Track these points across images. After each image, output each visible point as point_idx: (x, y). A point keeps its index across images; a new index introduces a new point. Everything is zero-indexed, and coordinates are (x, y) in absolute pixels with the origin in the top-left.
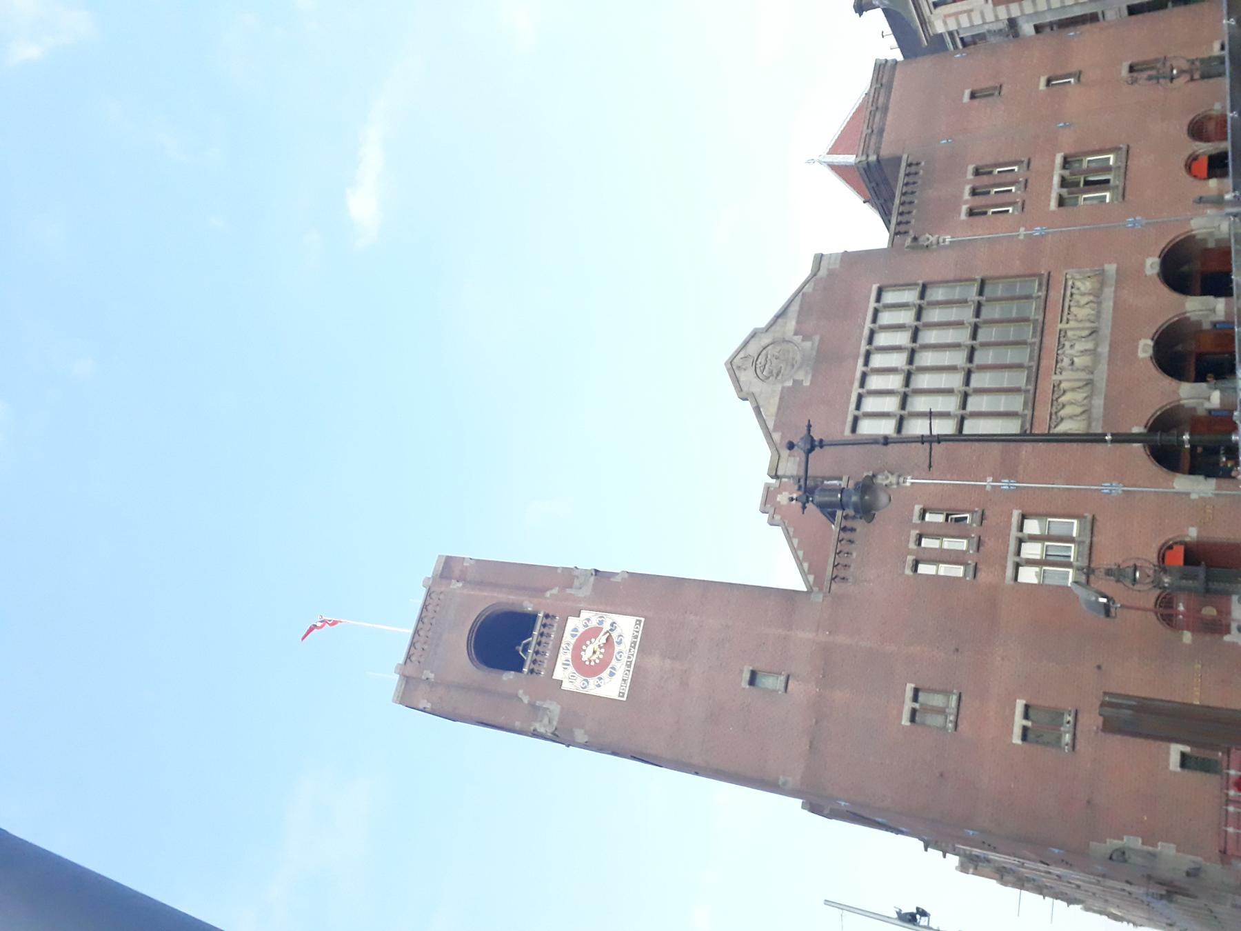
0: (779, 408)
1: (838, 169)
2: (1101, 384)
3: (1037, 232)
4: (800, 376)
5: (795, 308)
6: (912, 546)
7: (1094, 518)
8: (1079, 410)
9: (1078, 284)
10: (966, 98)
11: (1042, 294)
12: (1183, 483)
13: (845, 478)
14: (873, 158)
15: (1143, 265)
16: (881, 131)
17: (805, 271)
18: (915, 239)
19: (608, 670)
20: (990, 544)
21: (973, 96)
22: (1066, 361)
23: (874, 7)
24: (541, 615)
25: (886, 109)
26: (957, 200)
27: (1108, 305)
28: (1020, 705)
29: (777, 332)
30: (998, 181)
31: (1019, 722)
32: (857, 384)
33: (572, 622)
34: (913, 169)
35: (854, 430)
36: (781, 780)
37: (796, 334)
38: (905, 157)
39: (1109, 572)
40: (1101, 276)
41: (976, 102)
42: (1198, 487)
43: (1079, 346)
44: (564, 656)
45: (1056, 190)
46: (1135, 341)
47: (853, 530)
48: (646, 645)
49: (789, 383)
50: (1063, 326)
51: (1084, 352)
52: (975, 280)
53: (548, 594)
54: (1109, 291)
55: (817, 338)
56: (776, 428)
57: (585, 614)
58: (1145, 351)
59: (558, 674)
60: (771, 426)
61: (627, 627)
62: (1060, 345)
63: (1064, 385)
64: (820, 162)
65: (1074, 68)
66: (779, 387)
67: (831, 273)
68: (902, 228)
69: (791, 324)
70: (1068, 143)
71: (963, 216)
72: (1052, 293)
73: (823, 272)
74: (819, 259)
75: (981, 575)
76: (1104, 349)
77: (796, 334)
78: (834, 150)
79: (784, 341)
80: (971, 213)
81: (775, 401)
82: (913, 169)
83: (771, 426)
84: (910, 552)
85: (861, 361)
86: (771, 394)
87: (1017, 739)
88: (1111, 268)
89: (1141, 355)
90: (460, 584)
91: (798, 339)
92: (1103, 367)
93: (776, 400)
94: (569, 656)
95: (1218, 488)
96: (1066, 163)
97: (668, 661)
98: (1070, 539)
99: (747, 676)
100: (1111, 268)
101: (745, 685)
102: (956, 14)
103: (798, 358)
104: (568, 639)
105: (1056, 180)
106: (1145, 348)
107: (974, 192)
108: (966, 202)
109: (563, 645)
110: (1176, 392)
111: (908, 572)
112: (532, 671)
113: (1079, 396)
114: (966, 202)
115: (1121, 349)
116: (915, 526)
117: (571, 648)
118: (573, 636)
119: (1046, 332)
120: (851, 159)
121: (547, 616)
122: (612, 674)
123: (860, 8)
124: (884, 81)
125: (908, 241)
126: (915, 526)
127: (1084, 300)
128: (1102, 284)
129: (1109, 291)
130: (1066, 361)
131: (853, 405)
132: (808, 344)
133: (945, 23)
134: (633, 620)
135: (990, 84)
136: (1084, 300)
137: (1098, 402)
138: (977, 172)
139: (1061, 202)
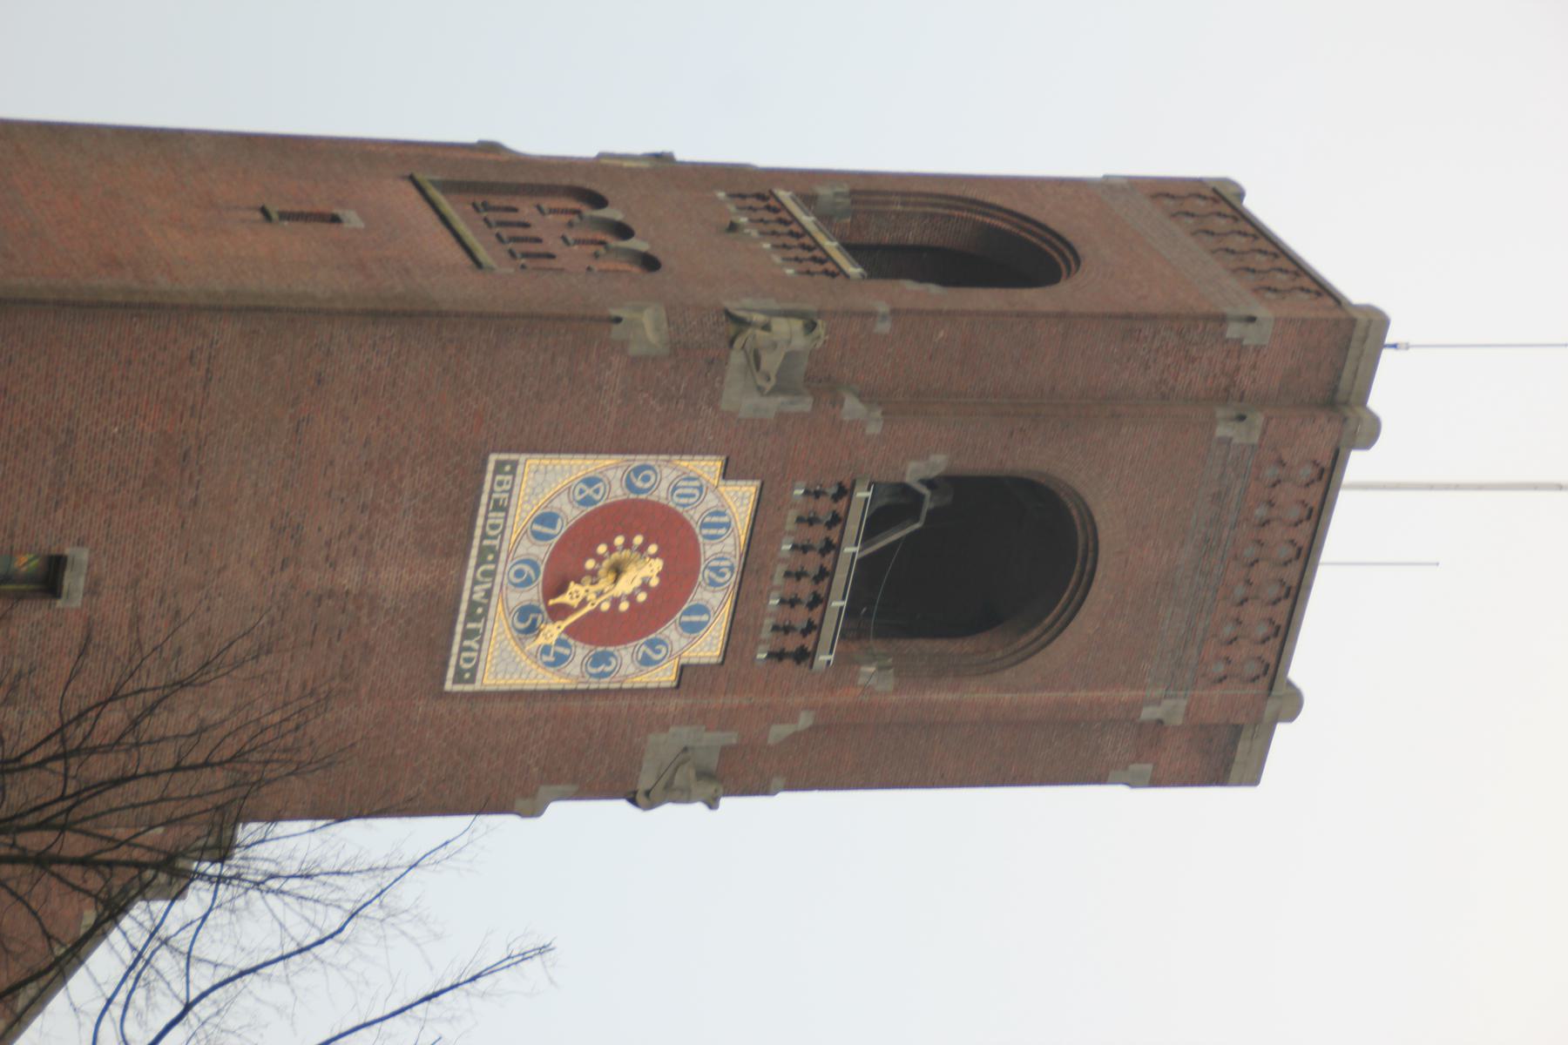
19: (560, 529)
24: (823, 658)
44: (723, 550)
48: (434, 622)
53: (805, 720)
57: (664, 675)
59: (740, 498)
61: (506, 657)
90: (1148, 713)
94: (709, 551)
97: (349, 577)
104: (715, 600)
109: (731, 579)
112: (844, 492)
117: (705, 574)
118: (701, 609)
121: (803, 656)
122: (547, 519)
134: (490, 679)
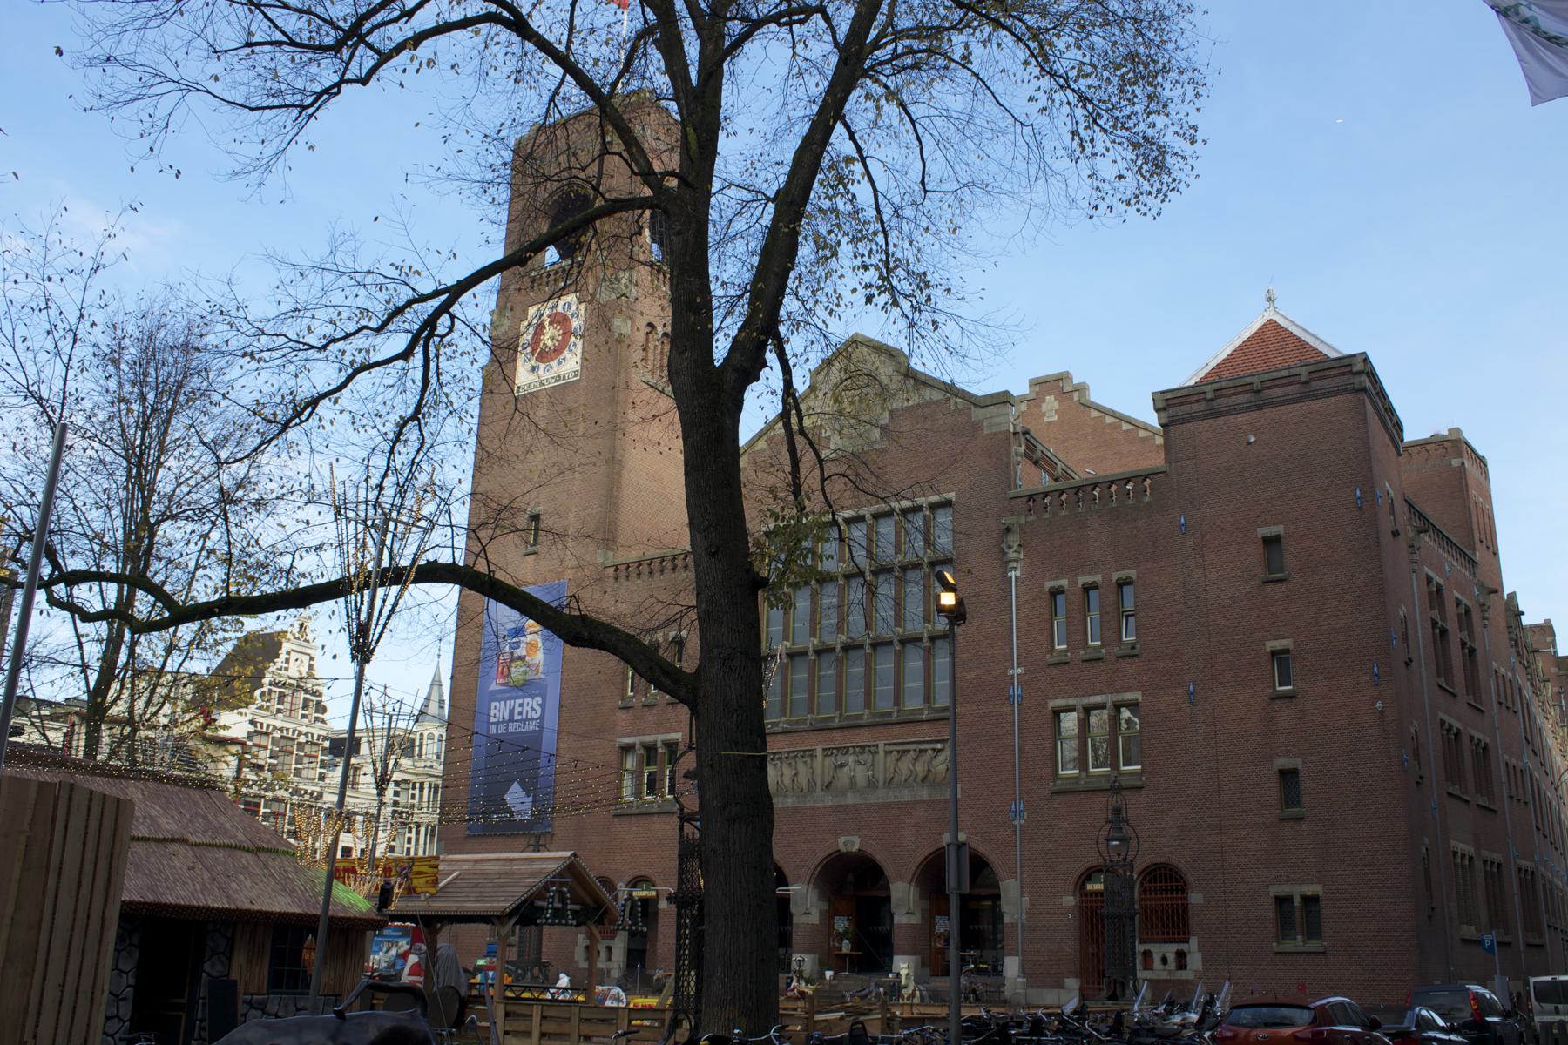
3: (1016, 690)
9: (942, 757)
20: (651, 717)
22: (841, 759)
27: (906, 796)
33: (571, 298)
51: (852, 779)
58: (845, 844)
67: (976, 427)
72: (925, 727)
75: (622, 715)
76: (851, 799)
77: (892, 413)
89: (841, 840)
92: (829, 800)
106: (851, 843)
110: (798, 880)
119: (875, 730)
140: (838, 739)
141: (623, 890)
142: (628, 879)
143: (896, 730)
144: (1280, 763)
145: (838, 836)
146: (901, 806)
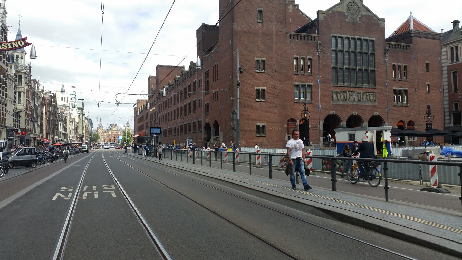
0: (339, 12)
1: (408, 22)
2: (346, 103)
4: (349, 18)
5: (369, 14)
6: (301, 57)
7: (312, 103)
8: (339, 98)
9: (372, 96)
10: (427, 62)
11: (370, 87)
12: (322, 123)
13: (318, 35)
14: (412, 35)
15: (377, 111)
16: (420, 37)
17: (380, 16)
18: (388, 50)
20: (303, 78)
21: (427, 64)
22: (351, 94)
23: (454, 27)
25: (427, 38)
26: (398, 61)
27: (367, 104)
28: (265, 88)
29: (362, 9)
30: (402, 73)
31: (261, 88)
32: (346, 36)
34: (408, 48)
35: (333, 36)
36: (235, 23)
37: (361, 15)
38: (412, 45)
39: (305, 108)
40: (375, 101)
41: (425, 65)
42: (321, 126)
43: (356, 98)
45: (398, 88)
46: (357, 111)
47: (304, 39)
49: (346, 15)
50: (361, 93)
52: (375, 68)
54: (370, 104)
55: (360, 22)
56: (333, 11)
60: (333, 10)
62: (356, 92)
63: (345, 95)
64: (410, 17)
65: (431, 91)
66: (345, 11)
67: (379, 25)
68: (391, 46)
69: (364, 13)
70: (411, 91)
71: (393, 63)
73: (379, 22)
74: (383, 20)
75: (295, 76)
76: (355, 103)
77: (361, 15)
78: (415, 21)
79: (359, 11)
80: (394, 66)
81: (341, 10)
82: (408, 48)
83: (333, 10)
84: (300, 56)
85: (353, 37)
86: (343, 9)
87: (256, 88)
88: (376, 104)
89: (353, 112)
91: (360, 16)
92: (351, 103)
93: (341, 11)
95: (321, 131)
96: (406, 91)
98: (299, 98)
99: (260, 9)
100: (376, 104)
101: (258, 9)
102: (447, 55)
103: (354, 17)
105: (401, 88)
106: (355, 113)
107: (400, 66)
108: (397, 64)
110: (344, 121)
111: (294, 56)
113: (342, 97)
114: (397, 64)
115: (354, 107)
116: (307, 57)
120: (412, 28)
123: (456, 23)
124: (436, 37)
125: (387, 48)
126: (307, 57)
127: (368, 98)
128: (372, 102)
129: (370, 104)
130: (351, 94)
131: (340, 35)
132: (358, 19)
133: (445, 51)
135: (430, 69)
136: (368, 98)
137: (341, 103)
138: (405, 67)
139: (395, 91)
140: (352, 90)
141: (298, 121)
142: (299, 119)
143: (364, 89)
144: (428, 104)
145: (352, 111)
146: (365, 106)
